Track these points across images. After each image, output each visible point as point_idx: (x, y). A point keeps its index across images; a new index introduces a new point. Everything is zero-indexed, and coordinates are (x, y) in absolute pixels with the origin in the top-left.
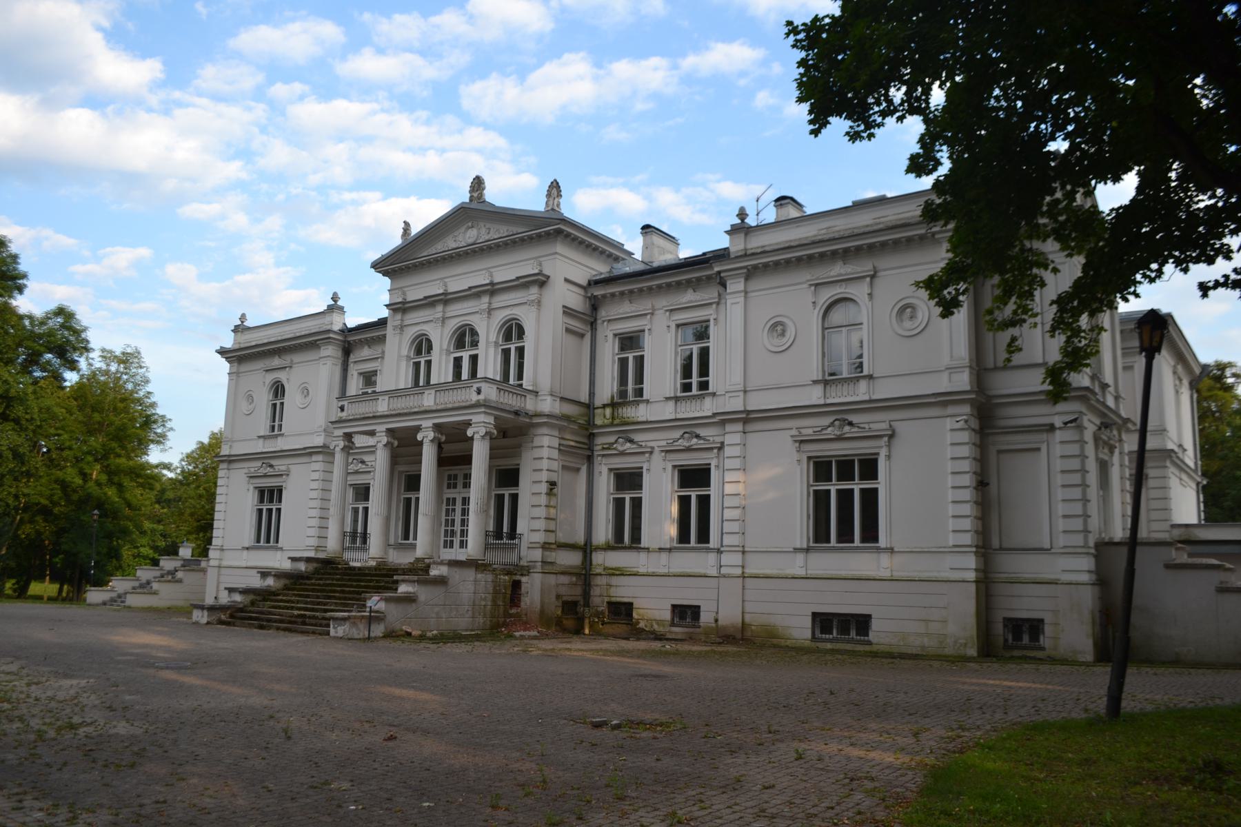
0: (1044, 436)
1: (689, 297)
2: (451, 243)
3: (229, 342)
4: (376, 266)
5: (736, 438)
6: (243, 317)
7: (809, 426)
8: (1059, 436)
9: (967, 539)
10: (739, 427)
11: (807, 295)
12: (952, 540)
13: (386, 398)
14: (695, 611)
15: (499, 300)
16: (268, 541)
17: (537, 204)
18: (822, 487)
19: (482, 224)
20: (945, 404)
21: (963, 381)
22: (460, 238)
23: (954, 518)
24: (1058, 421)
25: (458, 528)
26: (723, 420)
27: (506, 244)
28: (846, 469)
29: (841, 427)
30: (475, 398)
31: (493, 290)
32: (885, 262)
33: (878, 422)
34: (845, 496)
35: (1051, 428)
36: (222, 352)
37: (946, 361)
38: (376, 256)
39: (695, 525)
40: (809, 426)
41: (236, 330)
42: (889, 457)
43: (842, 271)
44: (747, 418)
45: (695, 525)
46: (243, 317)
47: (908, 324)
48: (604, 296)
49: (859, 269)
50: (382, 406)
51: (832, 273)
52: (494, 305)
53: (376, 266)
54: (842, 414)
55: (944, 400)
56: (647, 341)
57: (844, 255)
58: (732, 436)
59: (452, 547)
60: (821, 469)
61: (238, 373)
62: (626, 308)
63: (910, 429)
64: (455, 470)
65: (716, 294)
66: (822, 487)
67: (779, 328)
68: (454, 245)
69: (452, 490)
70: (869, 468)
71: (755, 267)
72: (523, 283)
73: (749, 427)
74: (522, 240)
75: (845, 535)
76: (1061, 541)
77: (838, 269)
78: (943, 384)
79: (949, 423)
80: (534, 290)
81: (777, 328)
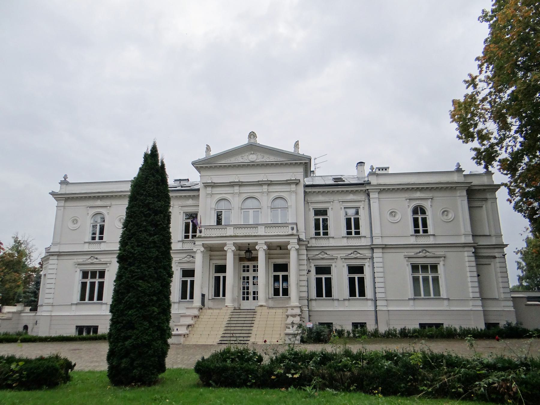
0: (492, 260)
1: (351, 197)
2: (239, 159)
3: (57, 189)
4: (193, 164)
5: (380, 255)
6: (65, 177)
7: (412, 252)
8: (497, 260)
9: (478, 295)
10: (381, 250)
11: (406, 203)
12: (471, 295)
13: (232, 228)
14: (363, 325)
15: (273, 188)
16: (91, 298)
17: (290, 149)
18: (416, 275)
19: (258, 154)
20: (464, 247)
21: (470, 240)
22: (246, 157)
23: (471, 288)
24: (497, 255)
25: (251, 290)
26: (372, 248)
27: (277, 164)
28: (425, 268)
29: (426, 252)
30: (290, 232)
31: (270, 183)
32: (437, 194)
33: (439, 252)
34: (426, 279)
35: (495, 257)
36: (53, 194)
37: (463, 232)
38: (196, 159)
39: (357, 288)
40: (412, 252)
41: (61, 183)
42: (444, 265)
43: (420, 196)
44: (385, 247)
45: (357, 288)
46: (65, 177)
47: (445, 217)
48: (309, 192)
49: (427, 196)
50: (230, 232)
51: (415, 196)
52: (270, 190)
53: (193, 164)
54: (425, 247)
55: (465, 245)
56: (330, 213)
57: (422, 190)
58: (378, 254)
59: (248, 299)
60: (415, 268)
61: (64, 206)
62: (321, 198)
63: (451, 255)
64: (247, 263)
65: (364, 197)
66: (416, 275)
67: (393, 214)
68: (242, 161)
69: (246, 273)
70: (434, 268)
71: (384, 189)
72: (288, 183)
73: (385, 251)
74: (286, 164)
75: (427, 293)
76: (503, 296)
77: (418, 195)
78: (463, 240)
79: (466, 254)
80: (293, 187)
81: (393, 213)
